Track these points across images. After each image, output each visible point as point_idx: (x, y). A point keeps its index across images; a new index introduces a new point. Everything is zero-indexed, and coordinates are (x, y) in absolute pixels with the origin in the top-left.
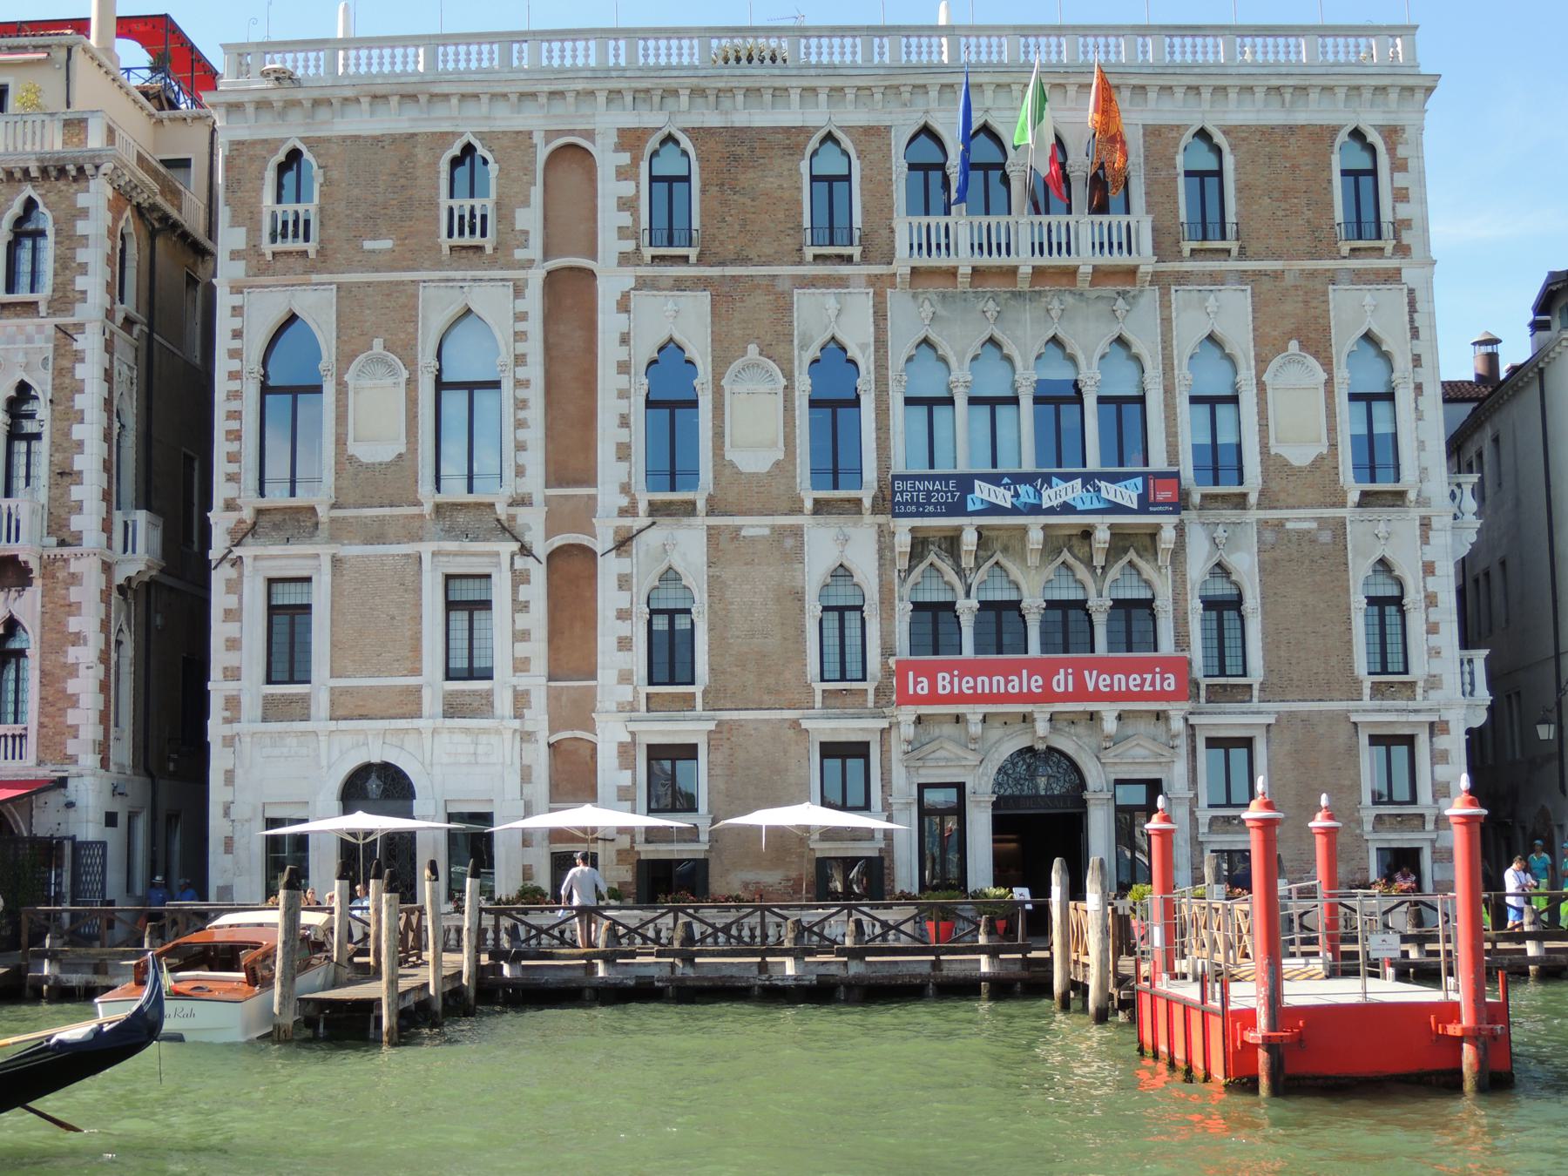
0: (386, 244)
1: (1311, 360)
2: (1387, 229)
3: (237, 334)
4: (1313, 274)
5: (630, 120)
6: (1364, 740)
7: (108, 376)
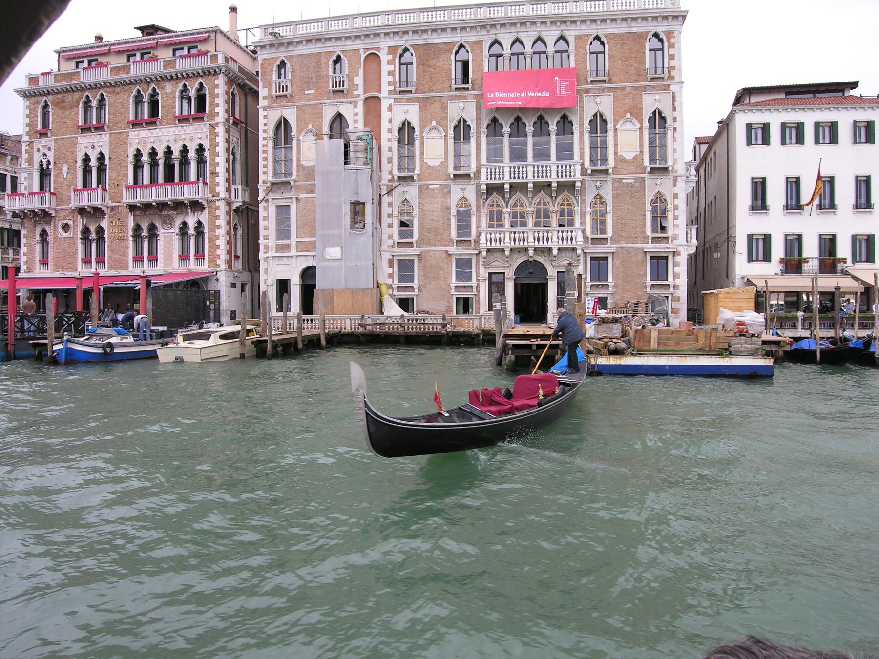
0: (312, 92)
1: (635, 121)
2: (666, 70)
3: (265, 125)
4: (636, 88)
5: (392, 44)
6: (648, 258)
7: (227, 141)
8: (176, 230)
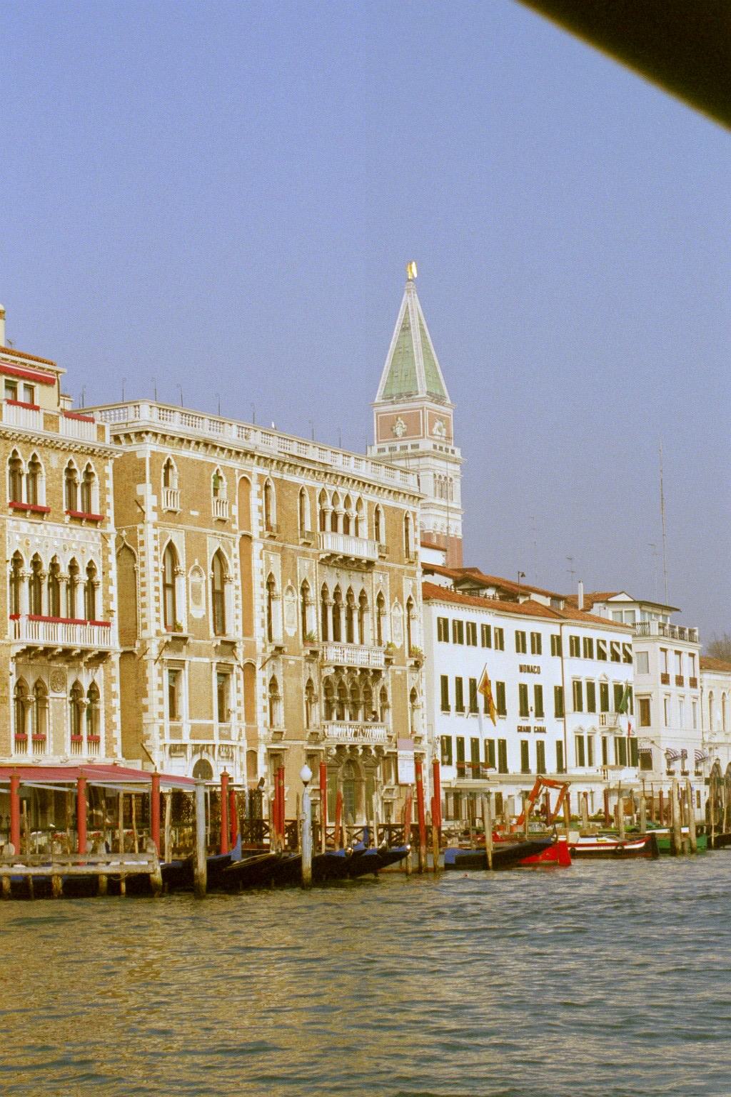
8: (65, 695)
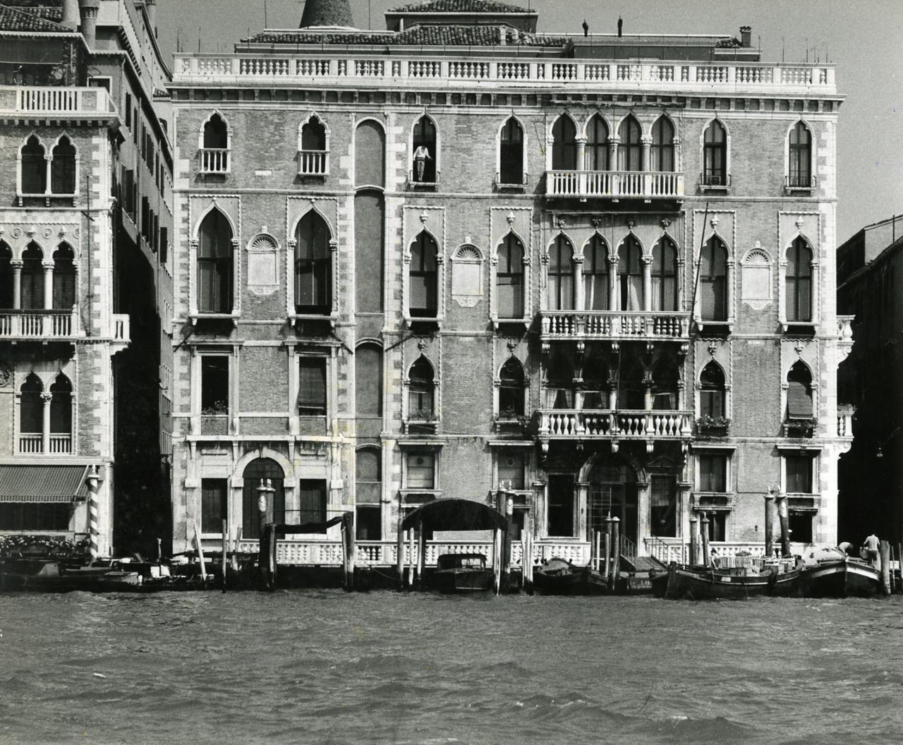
3: (186, 220)
